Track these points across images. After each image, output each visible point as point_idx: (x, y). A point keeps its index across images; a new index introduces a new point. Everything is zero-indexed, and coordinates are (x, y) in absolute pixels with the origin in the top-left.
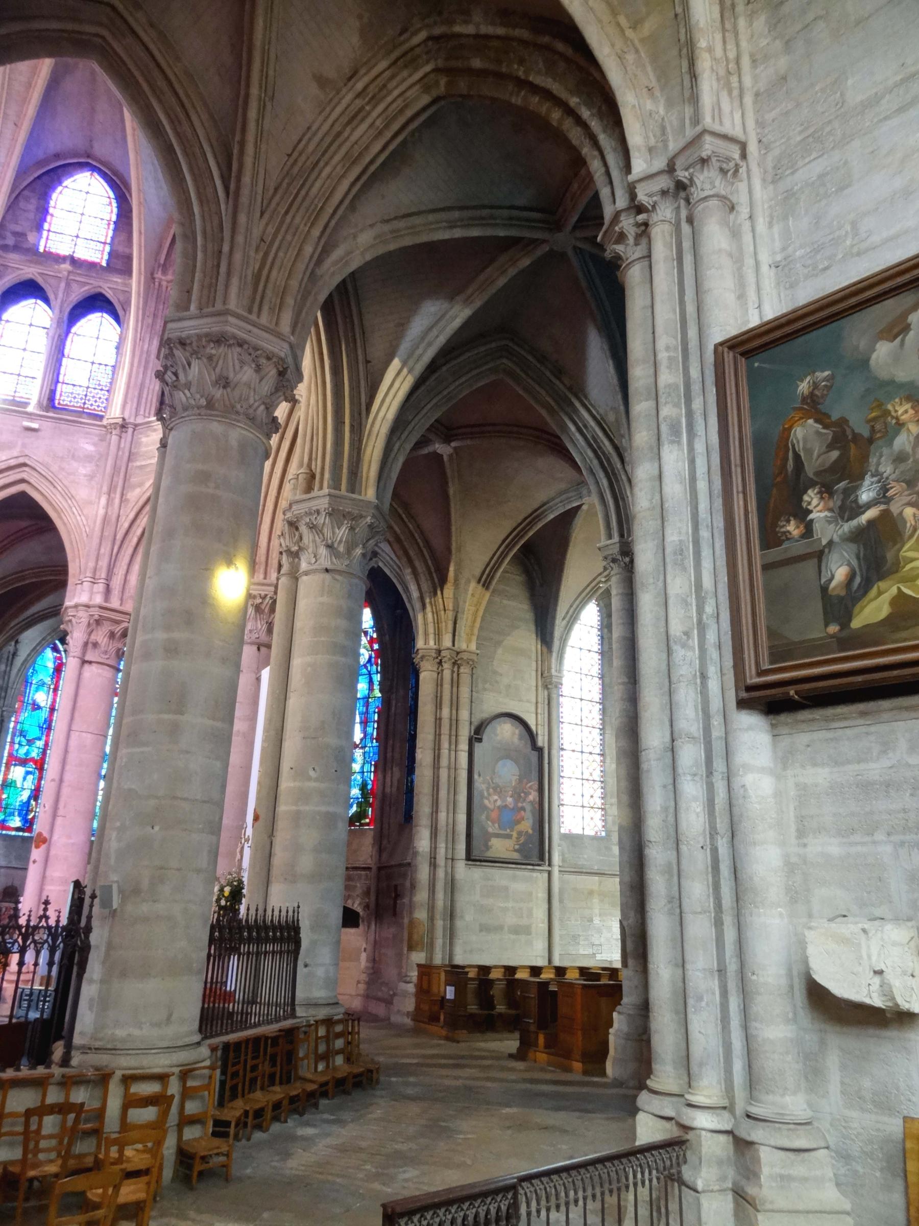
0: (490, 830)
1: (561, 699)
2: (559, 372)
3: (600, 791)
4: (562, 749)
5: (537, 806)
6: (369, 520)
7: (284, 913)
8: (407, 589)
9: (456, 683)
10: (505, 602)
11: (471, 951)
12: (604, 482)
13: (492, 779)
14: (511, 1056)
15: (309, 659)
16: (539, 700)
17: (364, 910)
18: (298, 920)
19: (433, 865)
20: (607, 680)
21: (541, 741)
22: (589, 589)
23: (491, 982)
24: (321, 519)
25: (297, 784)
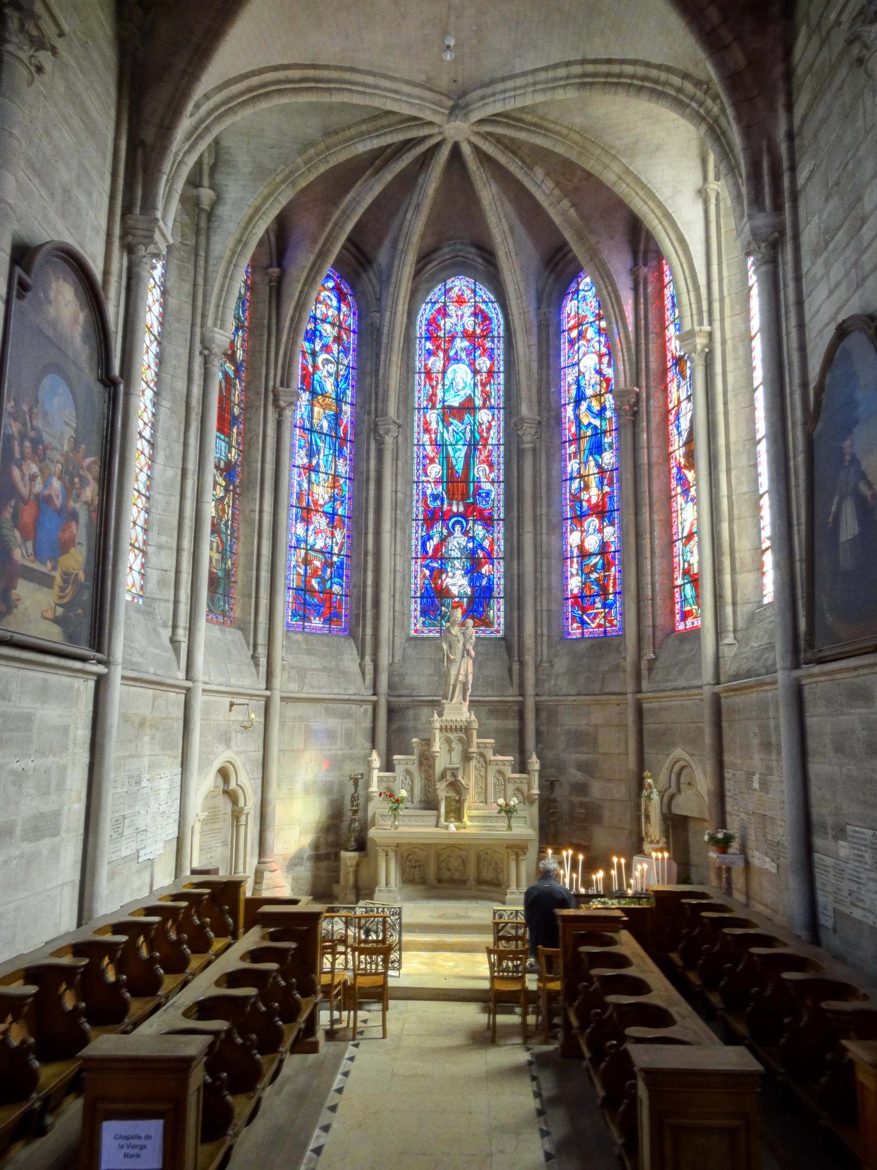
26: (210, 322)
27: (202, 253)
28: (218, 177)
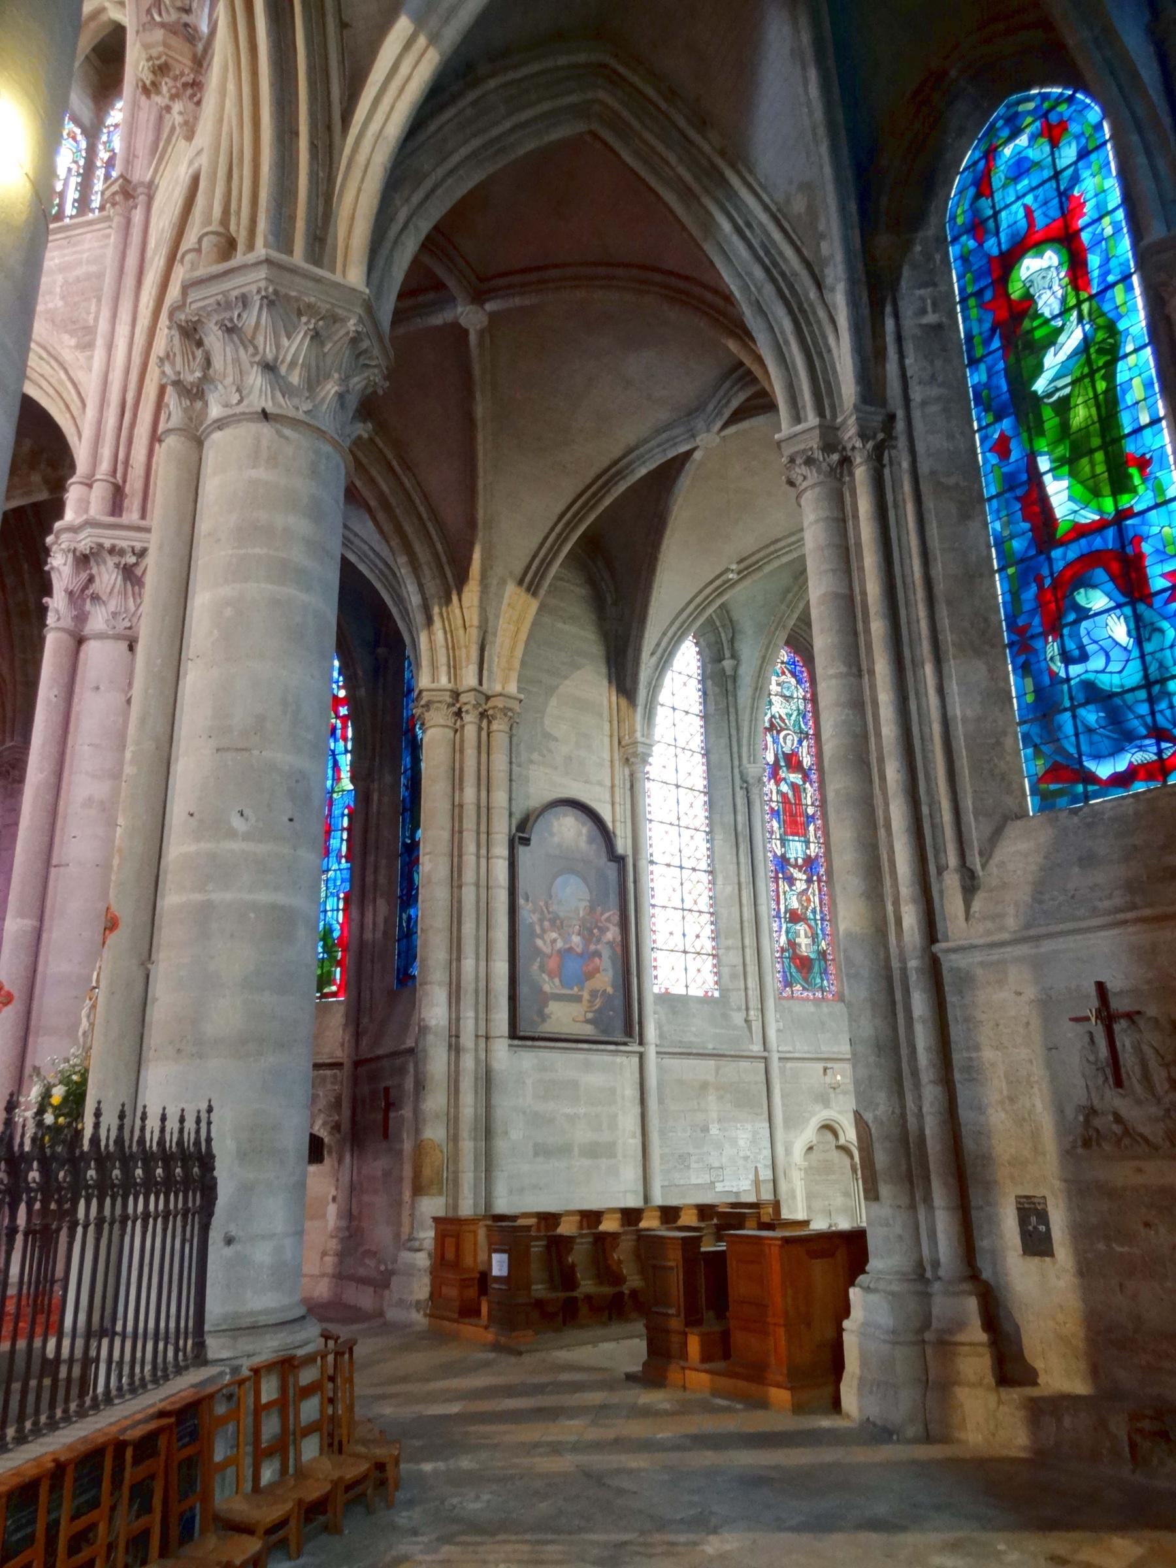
0: (547, 988)
1: (648, 785)
2: (703, 123)
3: (709, 928)
4: (652, 862)
5: (619, 950)
6: (352, 325)
7: (172, 1124)
8: (400, 600)
9: (484, 747)
10: (560, 625)
11: (522, 1190)
12: (787, 325)
13: (547, 904)
14: (630, 1378)
15: (227, 591)
16: (617, 782)
17: (331, 1133)
18: (209, 1140)
19: (455, 1048)
20: (714, 758)
21: (623, 845)
22: (692, 607)
23: (567, 1241)
24: (249, 319)
25: (206, 846)
26: (745, 760)
27: (732, 710)
28: (737, 644)
